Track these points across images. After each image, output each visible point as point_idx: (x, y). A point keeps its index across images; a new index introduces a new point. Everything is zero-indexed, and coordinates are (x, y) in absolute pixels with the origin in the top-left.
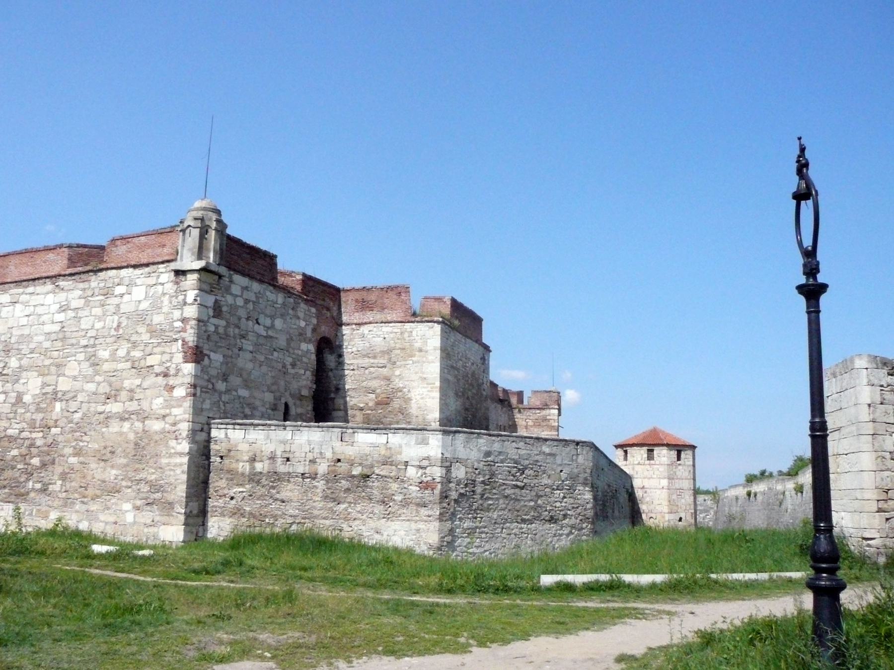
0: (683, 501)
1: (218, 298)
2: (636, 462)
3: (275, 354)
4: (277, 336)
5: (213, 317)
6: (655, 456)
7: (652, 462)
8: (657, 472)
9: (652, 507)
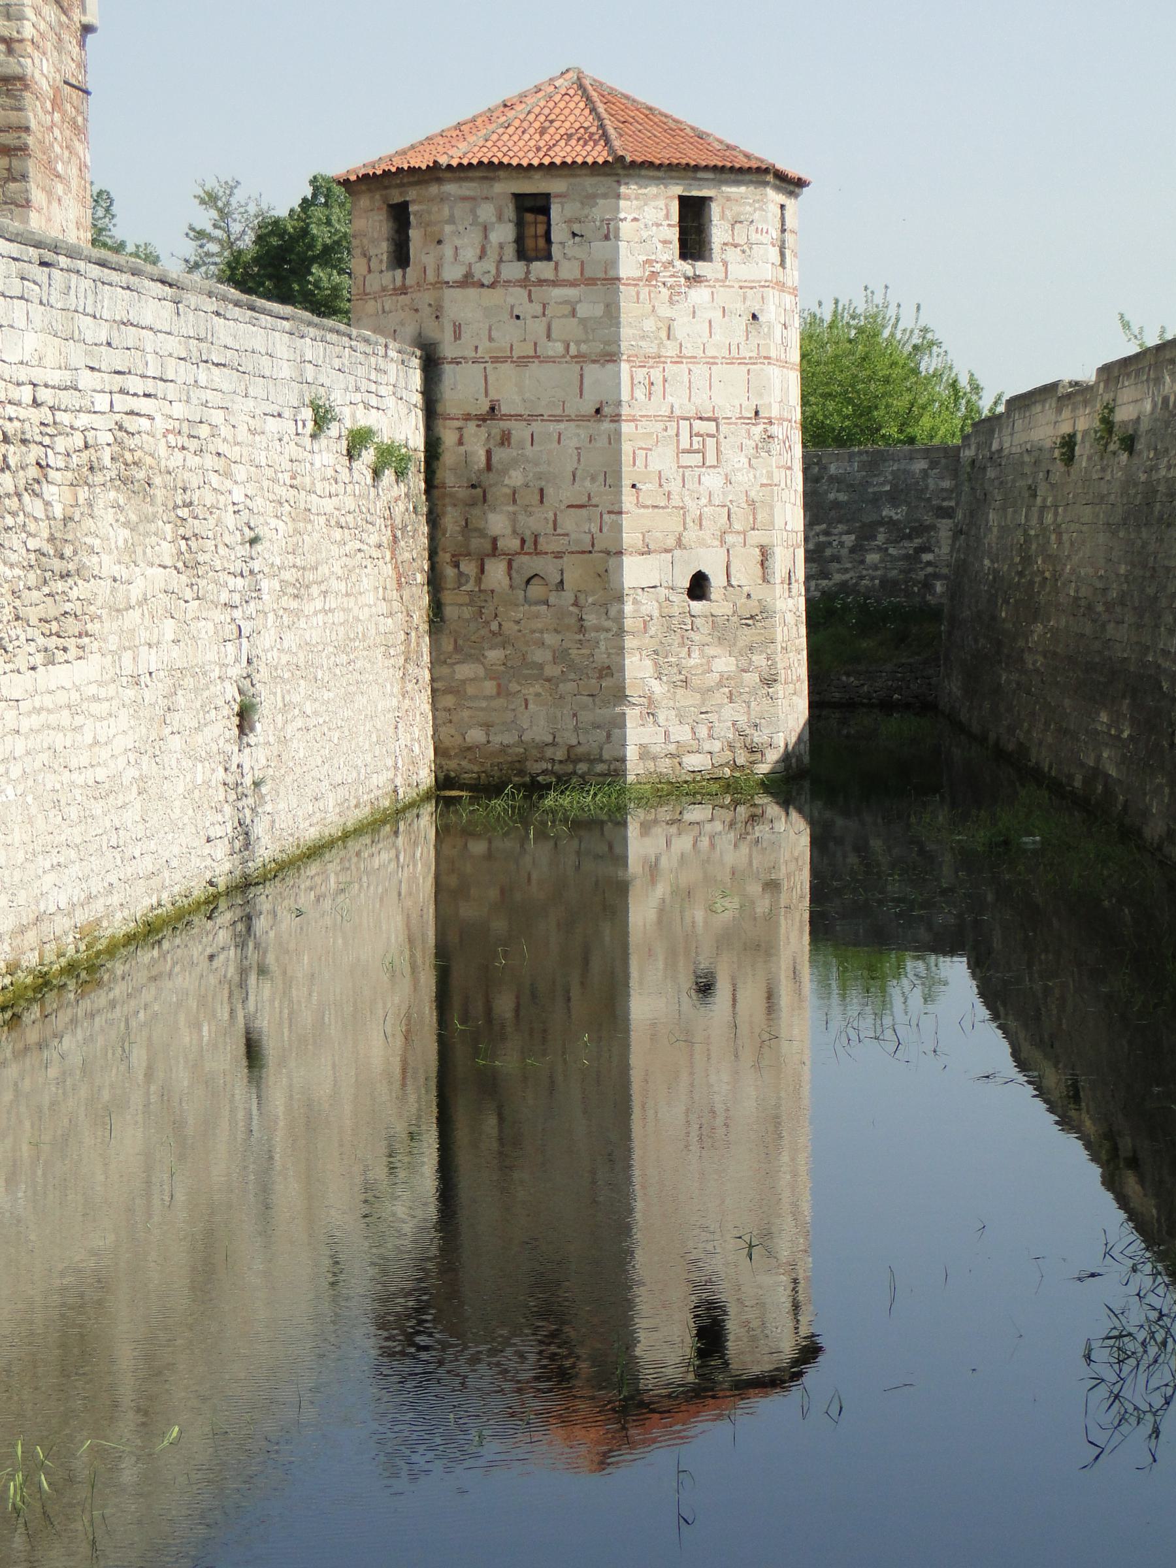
0: (712, 481)
2: (453, 273)
7: (540, 269)
8: (565, 327)
9: (536, 522)
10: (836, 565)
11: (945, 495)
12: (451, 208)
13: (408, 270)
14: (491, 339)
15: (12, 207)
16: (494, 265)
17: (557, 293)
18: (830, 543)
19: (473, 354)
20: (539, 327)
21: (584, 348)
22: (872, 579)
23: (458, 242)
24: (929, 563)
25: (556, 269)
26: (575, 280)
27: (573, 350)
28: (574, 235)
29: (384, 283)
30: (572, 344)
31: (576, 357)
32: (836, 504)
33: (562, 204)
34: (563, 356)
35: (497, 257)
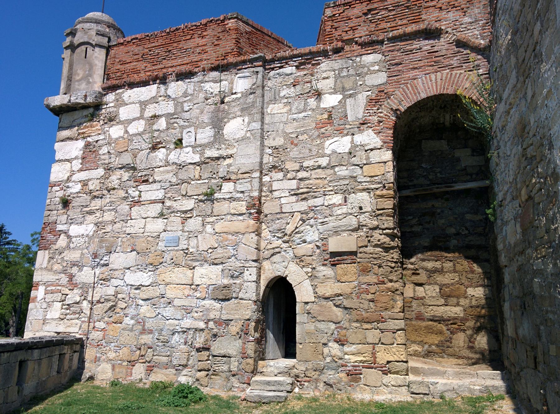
1: (89, 139)
3: (228, 187)
4: (230, 152)
5: (81, 170)
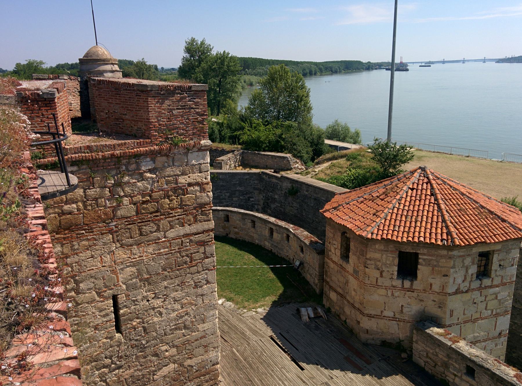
6: (495, 266)
7: (487, 282)
10: (224, 200)
11: (255, 184)
12: (454, 261)
13: (415, 282)
14: (464, 314)
15: (207, 271)
16: (468, 283)
17: (492, 291)
18: (222, 195)
19: (457, 322)
20: (482, 306)
21: (498, 311)
22: (236, 204)
23: (455, 276)
24: (253, 201)
25: (492, 281)
26: (499, 284)
27: (494, 313)
28: (500, 265)
29: (394, 283)
30: (494, 310)
31: (495, 315)
32: (222, 186)
33: (499, 254)
34: (491, 315)
35: (470, 280)
